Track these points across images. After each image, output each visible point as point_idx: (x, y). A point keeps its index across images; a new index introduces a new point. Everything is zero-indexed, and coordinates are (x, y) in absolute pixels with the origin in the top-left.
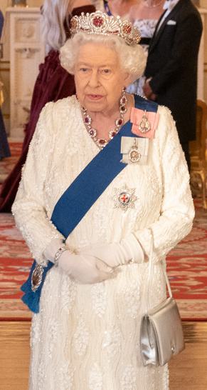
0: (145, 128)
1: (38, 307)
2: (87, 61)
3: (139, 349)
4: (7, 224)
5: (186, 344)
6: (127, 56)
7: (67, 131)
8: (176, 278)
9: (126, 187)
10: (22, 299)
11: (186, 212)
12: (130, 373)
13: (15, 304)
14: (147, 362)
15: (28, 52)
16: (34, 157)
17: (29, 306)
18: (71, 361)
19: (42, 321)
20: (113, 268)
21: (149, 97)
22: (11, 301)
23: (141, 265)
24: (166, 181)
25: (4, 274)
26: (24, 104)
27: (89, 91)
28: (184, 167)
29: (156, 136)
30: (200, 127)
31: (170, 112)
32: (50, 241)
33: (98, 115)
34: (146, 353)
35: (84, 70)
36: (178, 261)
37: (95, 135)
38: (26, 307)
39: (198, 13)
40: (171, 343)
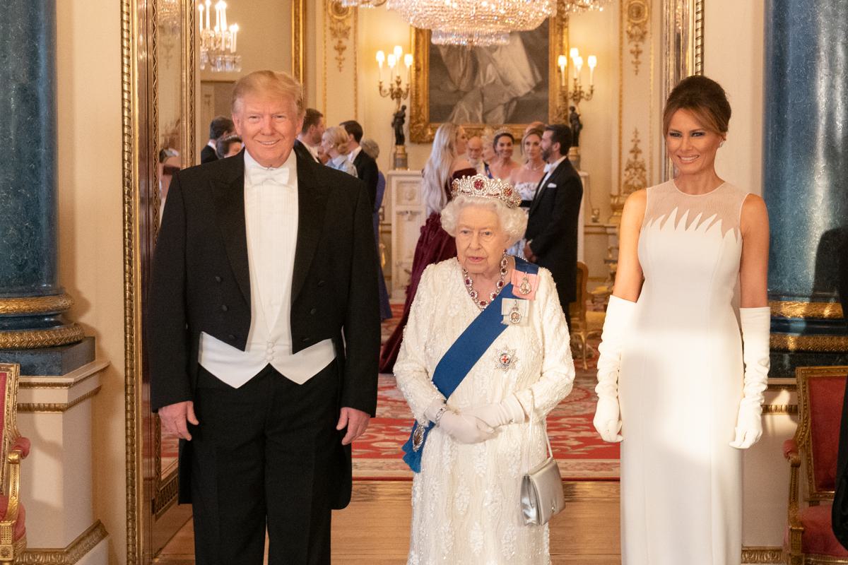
0: (527, 290)
1: (420, 467)
2: (467, 223)
3: (520, 509)
4: (389, 385)
5: (566, 503)
6: (508, 218)
7: (448, 293)
8: (556, 438)
9: (506, 348)
10: (404, 459)
11: (566, 373)
12: (510, 533)
13: (397, 464)
14: (528, 521)
15: (409, 214)
16: (416, 319)
17: (410, 466)
18: (452, 521)
19: (423, 480)
20: (494, 428)
21: (530, 259)
22: (393, 461)
23: (522, 425)
24: (546, 342)
25: (386, 434)
26: (405, 266)
27: (470, 253)
28: (564, 329)
29: (537, 297)
30: (581, 289)
31: (550, 274)
32: (431, 401)
33: (478, 277)
34: (527, 512)
35: (465, 232)
36: (559, 421)
37: (476, 296)
38: (408, 467)
39: (578, 175)
40: (552, 502)
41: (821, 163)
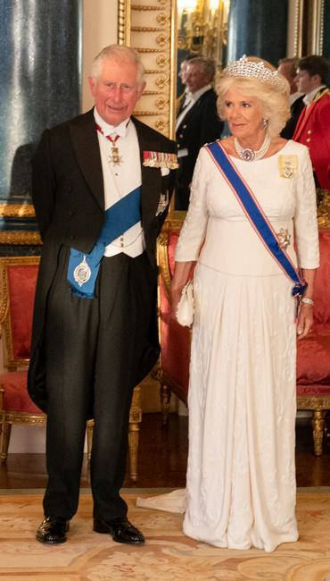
41: (17, 91)
